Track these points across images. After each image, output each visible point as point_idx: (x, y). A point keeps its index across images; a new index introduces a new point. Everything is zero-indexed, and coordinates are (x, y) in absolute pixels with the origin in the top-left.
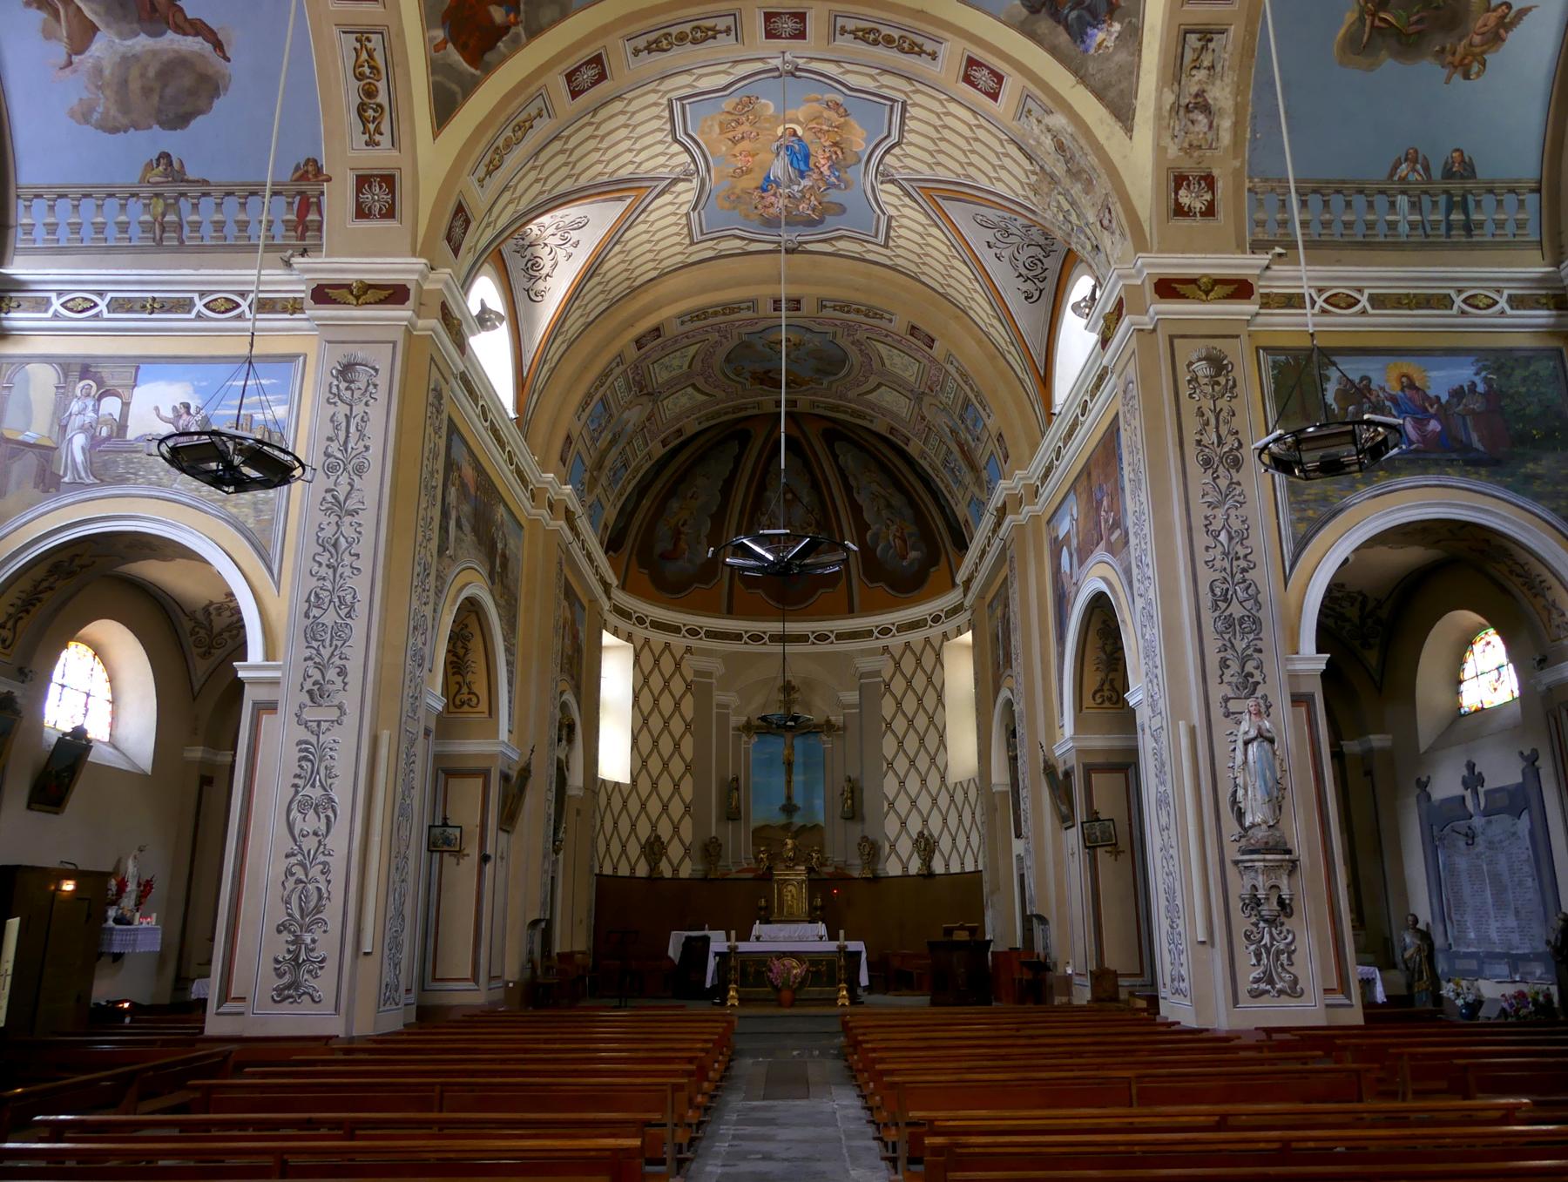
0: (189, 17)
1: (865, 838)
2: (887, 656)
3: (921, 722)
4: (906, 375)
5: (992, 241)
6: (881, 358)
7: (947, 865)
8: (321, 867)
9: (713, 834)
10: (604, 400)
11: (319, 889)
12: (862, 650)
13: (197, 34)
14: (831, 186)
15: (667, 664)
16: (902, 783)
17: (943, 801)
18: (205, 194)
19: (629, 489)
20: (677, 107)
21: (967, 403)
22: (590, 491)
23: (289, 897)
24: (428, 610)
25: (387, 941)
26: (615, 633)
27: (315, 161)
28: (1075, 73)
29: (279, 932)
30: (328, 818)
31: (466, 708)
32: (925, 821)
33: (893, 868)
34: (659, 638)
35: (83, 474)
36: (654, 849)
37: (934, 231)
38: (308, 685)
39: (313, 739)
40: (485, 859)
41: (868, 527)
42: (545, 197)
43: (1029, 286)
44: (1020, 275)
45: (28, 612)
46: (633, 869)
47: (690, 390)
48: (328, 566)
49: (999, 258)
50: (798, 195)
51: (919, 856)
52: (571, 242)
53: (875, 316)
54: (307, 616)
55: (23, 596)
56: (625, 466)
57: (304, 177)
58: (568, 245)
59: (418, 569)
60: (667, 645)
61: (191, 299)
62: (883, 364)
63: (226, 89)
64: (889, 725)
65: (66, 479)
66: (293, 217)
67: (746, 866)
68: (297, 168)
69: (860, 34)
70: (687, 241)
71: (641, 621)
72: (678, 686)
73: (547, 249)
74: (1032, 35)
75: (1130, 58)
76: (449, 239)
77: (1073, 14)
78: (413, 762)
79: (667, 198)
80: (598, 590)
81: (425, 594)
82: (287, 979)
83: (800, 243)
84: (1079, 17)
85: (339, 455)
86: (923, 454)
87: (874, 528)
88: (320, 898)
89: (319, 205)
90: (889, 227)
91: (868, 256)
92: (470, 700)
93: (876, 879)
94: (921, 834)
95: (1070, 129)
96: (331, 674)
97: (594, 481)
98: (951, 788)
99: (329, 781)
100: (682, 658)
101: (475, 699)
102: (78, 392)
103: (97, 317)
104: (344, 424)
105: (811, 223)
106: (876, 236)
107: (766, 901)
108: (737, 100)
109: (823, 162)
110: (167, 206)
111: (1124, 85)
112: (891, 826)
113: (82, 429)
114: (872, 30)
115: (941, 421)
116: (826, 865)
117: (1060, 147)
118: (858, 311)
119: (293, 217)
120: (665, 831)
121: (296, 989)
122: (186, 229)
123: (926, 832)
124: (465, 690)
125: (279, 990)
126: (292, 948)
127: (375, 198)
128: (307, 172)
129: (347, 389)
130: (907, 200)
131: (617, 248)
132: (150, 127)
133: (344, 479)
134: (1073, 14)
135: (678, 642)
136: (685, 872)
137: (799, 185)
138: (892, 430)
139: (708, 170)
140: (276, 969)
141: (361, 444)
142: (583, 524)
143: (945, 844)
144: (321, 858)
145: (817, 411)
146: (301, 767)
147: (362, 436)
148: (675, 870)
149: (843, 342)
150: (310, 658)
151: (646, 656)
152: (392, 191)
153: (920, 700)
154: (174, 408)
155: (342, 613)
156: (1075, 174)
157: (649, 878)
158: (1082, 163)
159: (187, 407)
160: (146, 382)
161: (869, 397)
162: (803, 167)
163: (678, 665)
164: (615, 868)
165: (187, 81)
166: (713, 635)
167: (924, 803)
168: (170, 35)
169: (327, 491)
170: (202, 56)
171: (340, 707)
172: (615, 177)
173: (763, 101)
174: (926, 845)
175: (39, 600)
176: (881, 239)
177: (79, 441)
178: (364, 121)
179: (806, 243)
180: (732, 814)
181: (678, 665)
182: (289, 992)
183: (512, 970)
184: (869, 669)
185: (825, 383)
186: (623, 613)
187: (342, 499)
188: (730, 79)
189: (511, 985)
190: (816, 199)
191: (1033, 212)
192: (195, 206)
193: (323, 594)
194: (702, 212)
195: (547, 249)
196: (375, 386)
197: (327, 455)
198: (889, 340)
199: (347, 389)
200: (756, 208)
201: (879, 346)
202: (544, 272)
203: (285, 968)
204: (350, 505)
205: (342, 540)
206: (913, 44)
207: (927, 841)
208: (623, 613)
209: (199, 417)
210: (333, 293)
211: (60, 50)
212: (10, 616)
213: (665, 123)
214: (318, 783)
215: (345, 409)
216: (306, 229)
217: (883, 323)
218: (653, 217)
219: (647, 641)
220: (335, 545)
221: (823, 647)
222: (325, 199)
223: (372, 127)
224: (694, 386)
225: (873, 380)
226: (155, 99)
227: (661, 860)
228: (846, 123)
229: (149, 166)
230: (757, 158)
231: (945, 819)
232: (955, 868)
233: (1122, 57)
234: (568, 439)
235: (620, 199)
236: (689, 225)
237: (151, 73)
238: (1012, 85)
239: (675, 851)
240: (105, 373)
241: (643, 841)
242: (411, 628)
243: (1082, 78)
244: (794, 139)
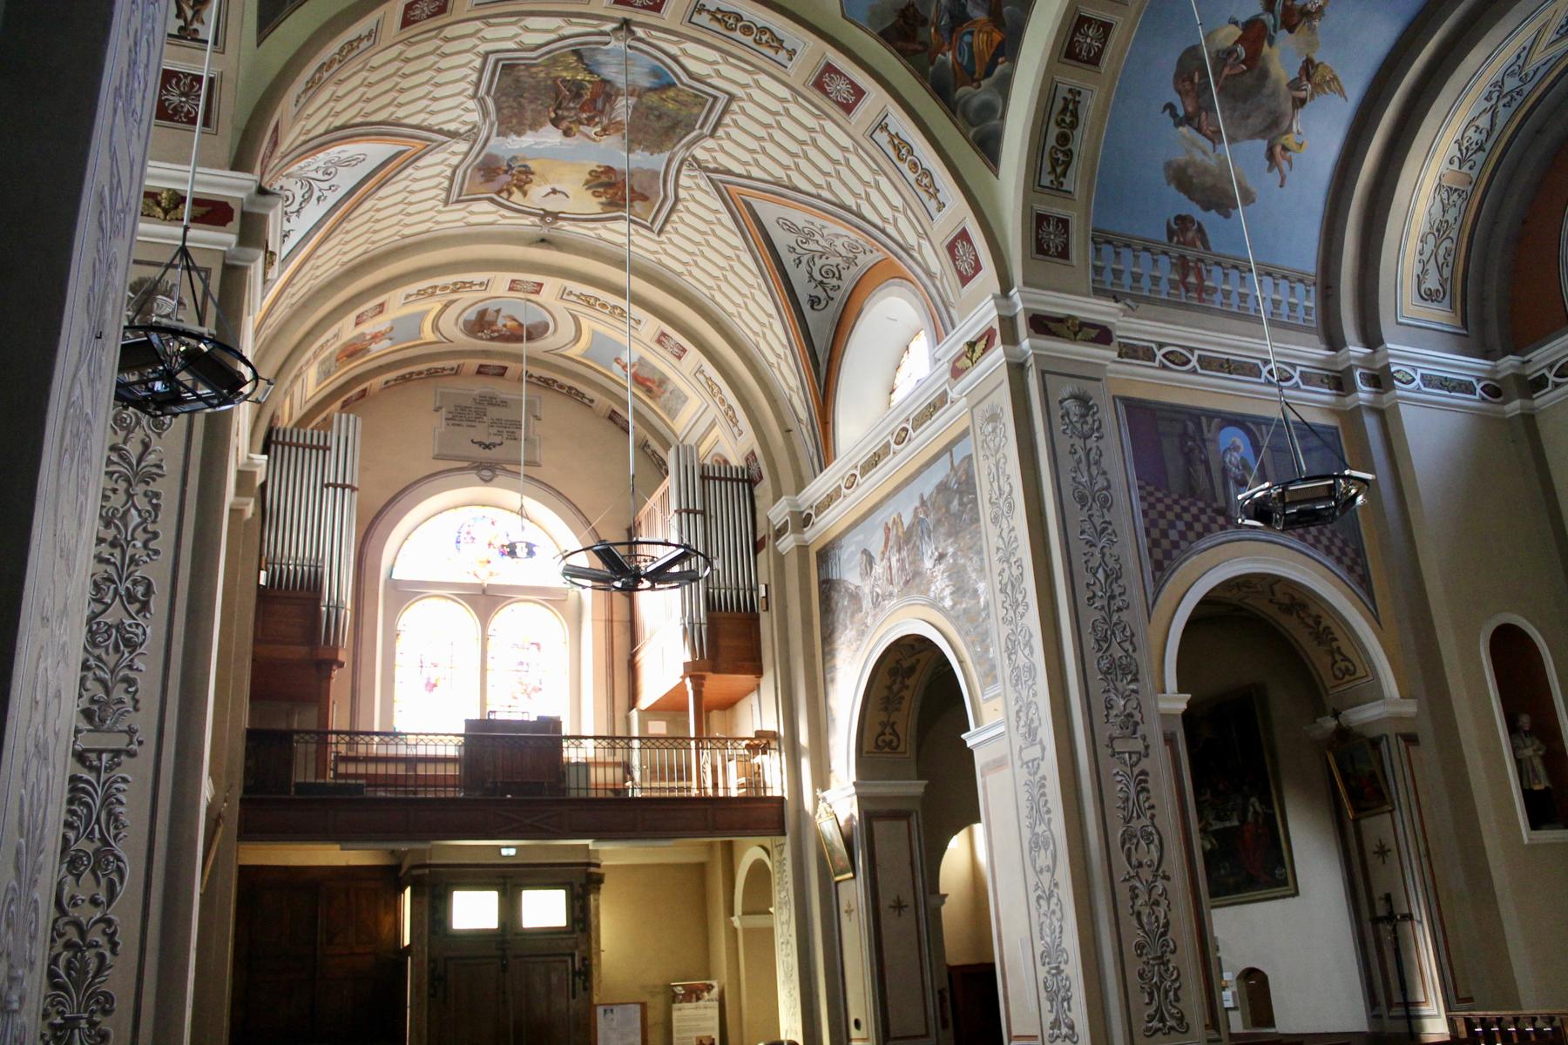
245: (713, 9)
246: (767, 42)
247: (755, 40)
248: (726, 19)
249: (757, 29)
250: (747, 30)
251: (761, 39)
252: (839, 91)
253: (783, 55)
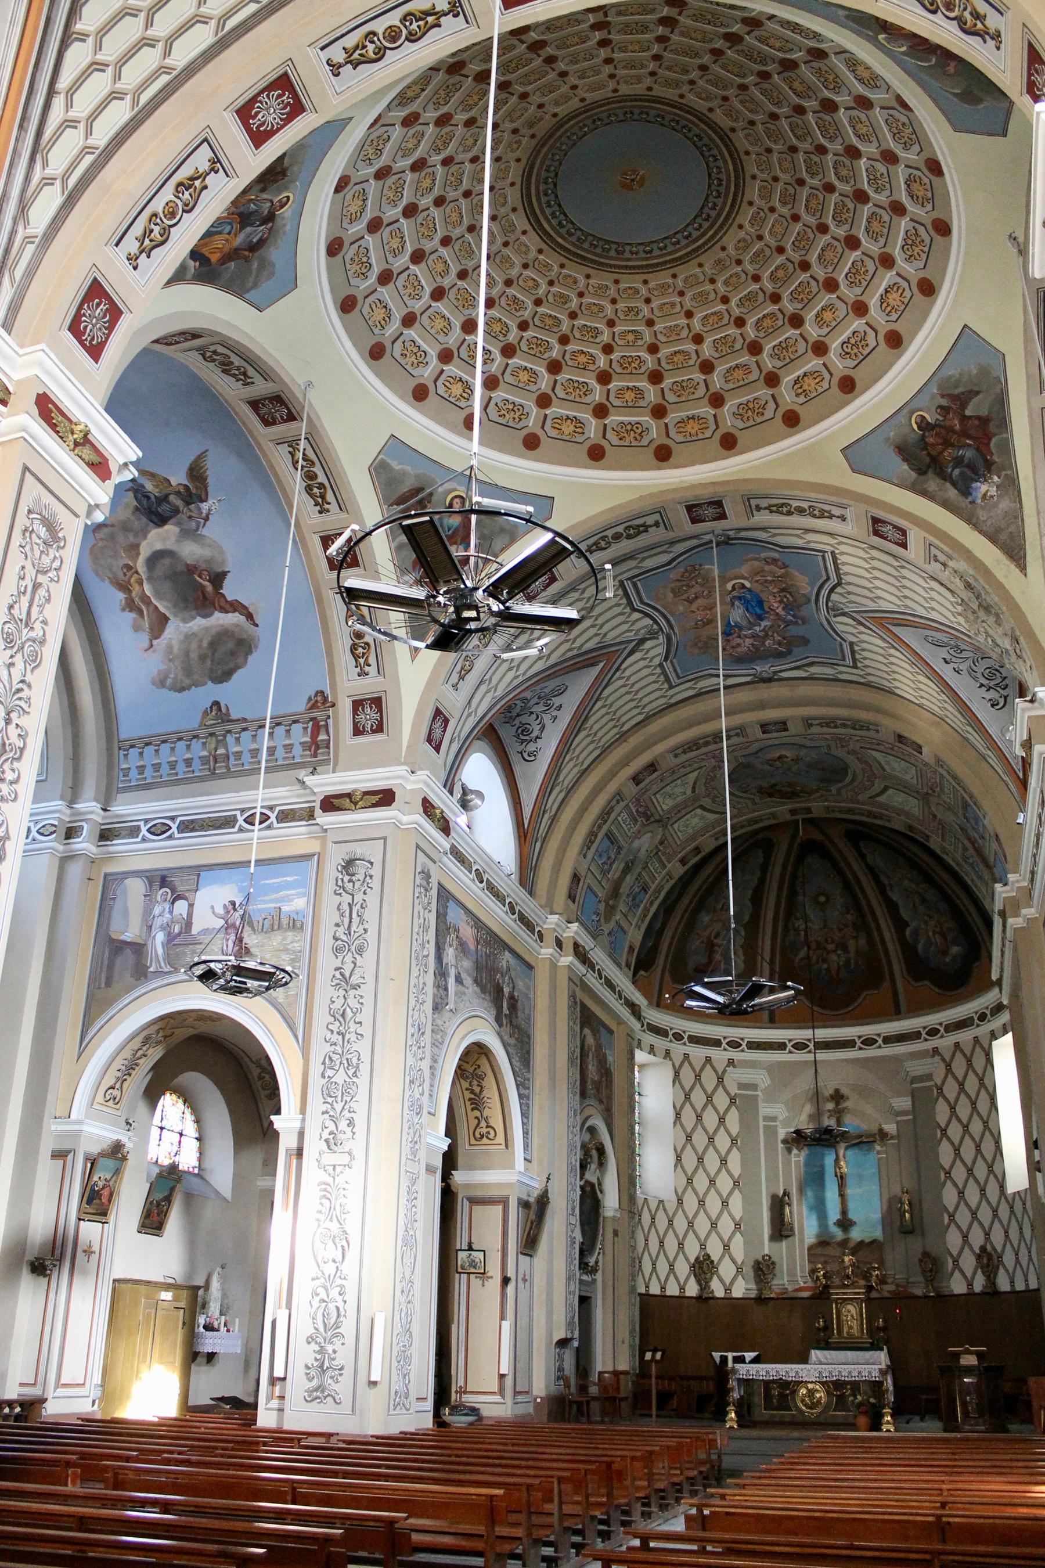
0: (229, 599)
1: (926, 1255)
2: (937, 1058)
3: (976, 1127)
4: (908, 777)
5: (948, 657)
6: (880, 764)
7: (1012, 1282)
8: (339, 1289)
9: (766, 1252)
10: (610, 836)
11: (338, 1308)
12: (911, 1053)
13: (234, 612)
14: (788, 623)
15: (709, 1079)
16: (961, 1193)
17: (1004, 1212)
18: (244, 729)
19: (653, 909)
20: (629, 586)
21: (966, 806)
22: (607, 920)
23: (315, 1313)
24: (425, 1065)
25: (395, 1354)
26: (652, 1050)
27: (322, 692)
28: (968, 521)
29: (309, 1343)
30: (343, 1247)
31: (485, 1140)
32: (987, 1234)
33: (958, 1286)
34: (697, 1053)
35: (163, 965)
36: (703, 1268)
37: (892, 651)
38: (326, 1135)
39: (330, 1180)
40: (506, 1281)
41: (906, 924)
42: (521, 679)
43: (992, 694)
44: (982, 685)
45: (130, 1075)
46: (682, 1288)
47: (699, 811)
48: (338, 1033)
50: (762, 634)
51: (983, 1273)
53: (861, 728)
54: (323, 1076)
55: (126, 1062)
56: (645, 889)
57: (314, 707)
59: (411, 1030)
60: (708, 1060)
61: (235, 816)
62: (884, 770)
63: (256, 647)
64: (944, 1132)
65: (151, 969)
66: (308, 739)
67: (802, 1284)
68: (310, 699)
69: (774, 509)
70: (666, 686)
71: (678, 1037)
72: (721, 1100)
73: (534, 716)
74: (924, 493)
75: (1012, 505)
76: (429, 740)
77: (957, 472)
78: (415, 1198)
79: (638, 655)
80: (625, 1013)
81: (420, 1051)
82: (315, 1383)
83: (775, 673)
84: (962, 474)
85: (344, 938)
86: (943, 849)
87: (913, 925)
88: (339, 1316)
89: (326, 726)
90: (853, 652)
91: (841, 677)
92: (488, 1133)
93: (944, 1299)
94: (983, 1249)
95: (971, 572)
96: (343, 1125)
97: (610, 910)
98: (1010, 1199)
99: (343, 1216)
100: (725, 1071)
101: (492, 1132)
102: (159, 899)
103: (170, 837)
104: (348, 912)
105: (780, 655)
106: (844, 659)
107: (825, 1322)
108: (682, 570)
109: (776, 605)
110: (218, 742)
111: (1012, 528)
112: (953, 1240)
113: (162, 928)
114: (782, 505)
115: (950, 818)
116: (886, 1283)
117: (968, 586)
118: (844, 726)
119: (308, 739)
120: (715, 1250)
121: (323, 1392)
122: (232, 758)
123: (989, 1247)
124: (483, 1124)
125: (310, 1392)
126: (319, 1357)
127: (368, 716)
128: (317, 701)
129: (349, 881)
131: (599, 704)
132: (205, 684)
133: (349, 959)
134: (957, 472)
135: (719, 1056)
136: (739, 1291)
138: (911, 828)
139: (671, 627)
140: (307, 1374)
141: (361, 927)
142: (598, 956)
143: (1009, 1259)
144: (338, 1282)
145: (832, 815)
146: (322, 1204)
147: (362, 921)
148: (728, 1290)
149: (840, 753)
150: (327, 1112)
151: (687, 1076)
152: (380, 710)
153: (973, 1104)
154: (225, 906)
155: (350, 1073)
156: (987, 609)
157: (699, 1298)
158: (988, 600)
159: (233, 903)
160: (204, 887)
161: (878, 799)
162: (759, 611)
163: (720, 1079)
164: (663, 1288)
165: (230, 645)
166: (753, 1045)
167: (985, 1215)
168: (217, 614)
169: (337, 969)
170: (237, 626)
171: (350, 1153)
172: (584, 649)
173: (707, 567)
174: (989, 1262)
175: (137, 1065)
176: (849, 661)
177: (160, 937)
178: (356, 657)
180: (781, 1229)
181: (720, 1079)
182: (317, 1394)
183: (541, 1385)
184: (919, 1073)
185: (834, 792)
186: (659, 1031)
187: (347, 975)
188: (671, 556)
189: (539, 1400)
191: (969, 636)
192: (238, 739)
193: (335, 1057)
195: (534, 716)
196: (371, 877)
197: (336, 939)
198: (881, 748)
199: (349, 881)
201: (874, 753)
202: (534, 735)
203: (313, 1373)
204: (354, 980)
205: (348, 1010)
206: (822, 511)
207: (990, 1256)
208: (659, 1031)
209: (241, 912)
210: (336, 802)
211: (144, 638)
212: (118, 1079)
213: (621, 599)
214: (334, 1218)
215: (347, 898)
216: (318, 747)
217: (872, 734)
218: (628, 673)
219: (686, 1056)
220: (343, 1015)
221: (871, 1052)
222: (331, 722)
223: (362, 661)
224: (701, 807)
225: (878, 786)
226: (209, 662)
227: (711, 1278)
228: (787, 573)
229: (206, 713)
231: (1006, 1232)
232: (1020, 1286)
233: (1005, 504)
234: (576, 878)
235: (593, 665)
236: (664, 673)
237: (205, 644)
238: (915, 536)
239: (726, 1270)
240: (177, 881)
241: (692, 1260)
242: (407, 1081)
243: (976, 526)
245: (443, 19)
246: (364, 47)
247: (374, 34)
248: (421, 23)
249: (386, 48)
250: (393, 34)
251: (372, 42)
252: (267, 109)
253: (340, 57)
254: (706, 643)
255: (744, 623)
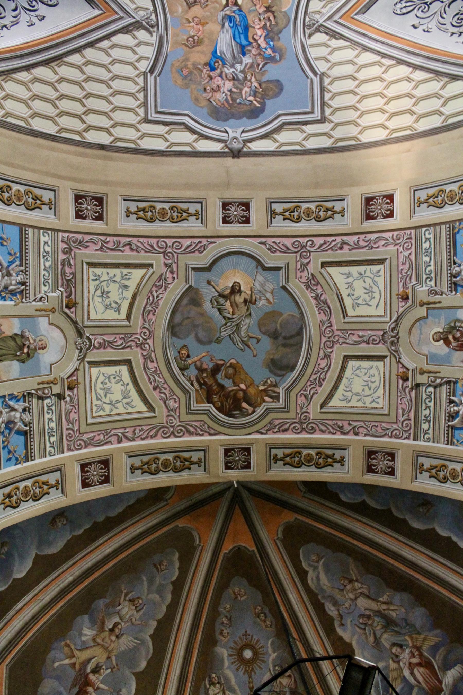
5: (416, 21)
44: (453, 34)
49: (428, 31)
52: (37, 13)
58: (32, 13)
90: (323, 89)
109: (259, 32)
130: (335, 43)
137: (241, 63)
139: (166, 29)
162: (244, 42)
179: (250, 141)
190: (257, 80)
194: (158, 79)
200: (205, 89)
218: (116, 53)
230: (207, 27)
244: (235, 8)
254: (190, 73)
255: (228, 56)
